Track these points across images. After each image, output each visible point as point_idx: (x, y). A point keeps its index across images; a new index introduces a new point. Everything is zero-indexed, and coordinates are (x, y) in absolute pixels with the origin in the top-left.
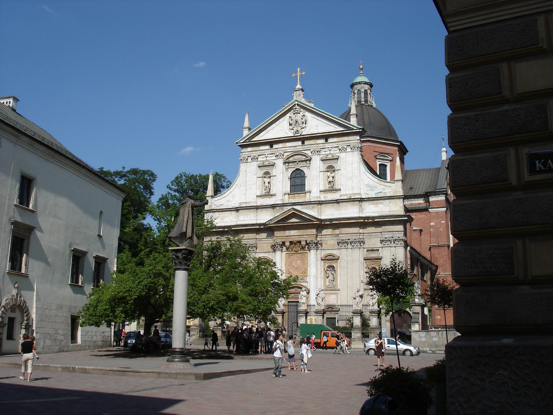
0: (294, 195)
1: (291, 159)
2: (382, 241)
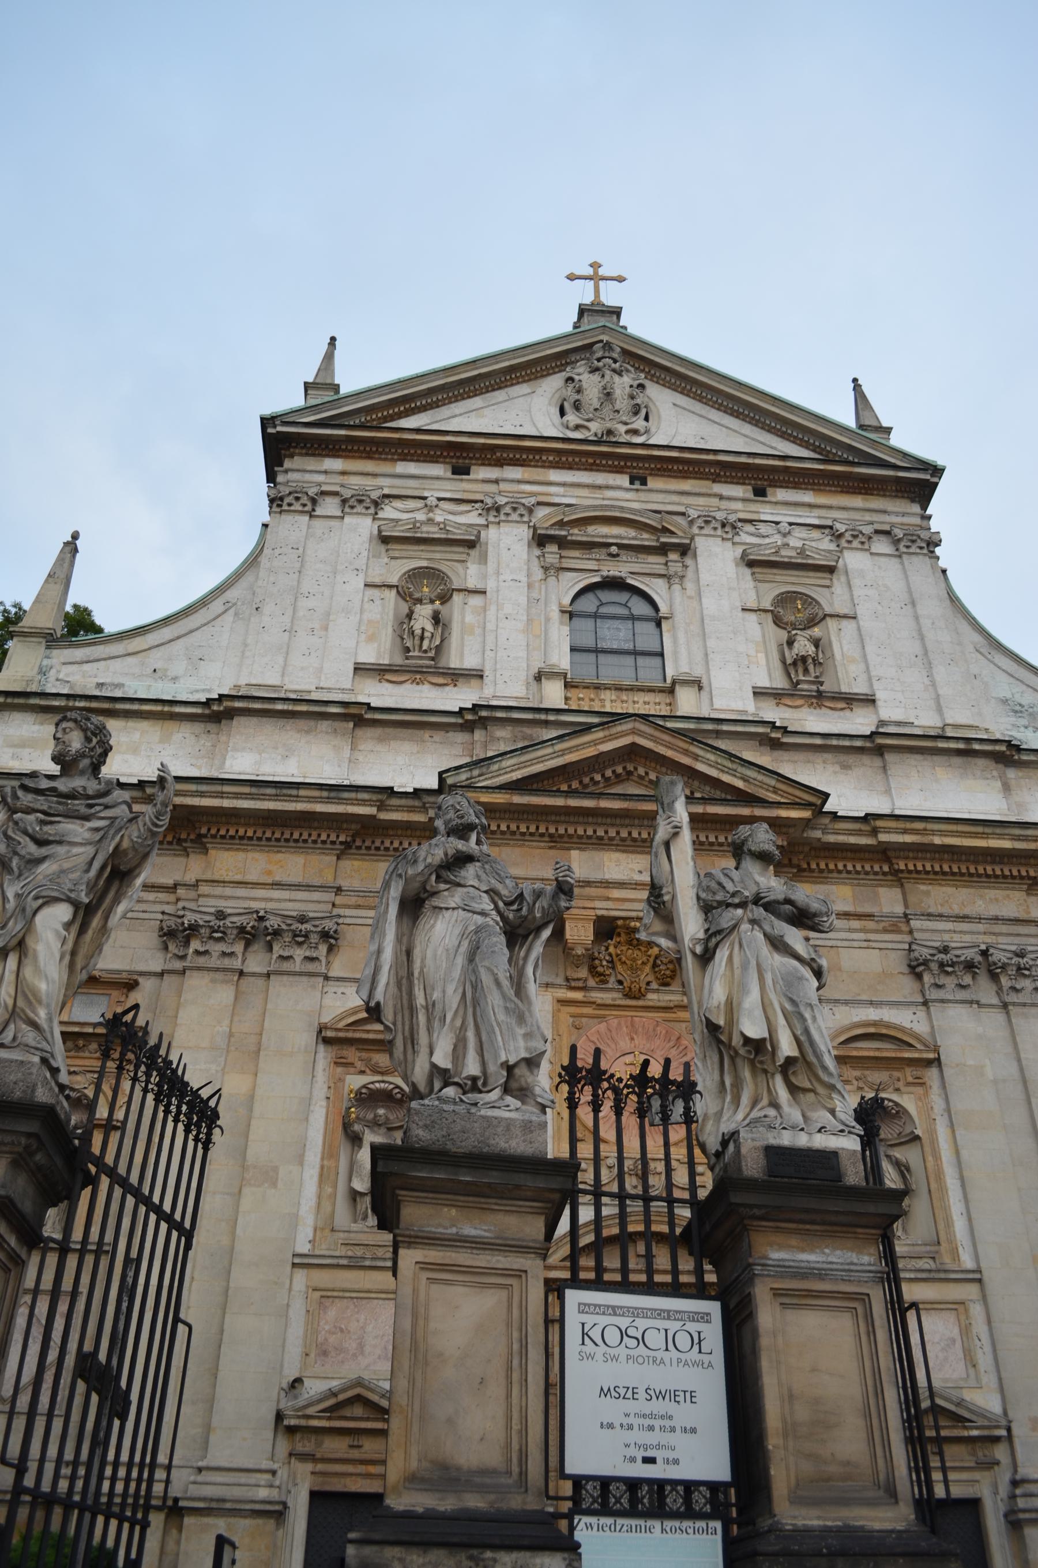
0: (597, 695)
1: (576, 534)
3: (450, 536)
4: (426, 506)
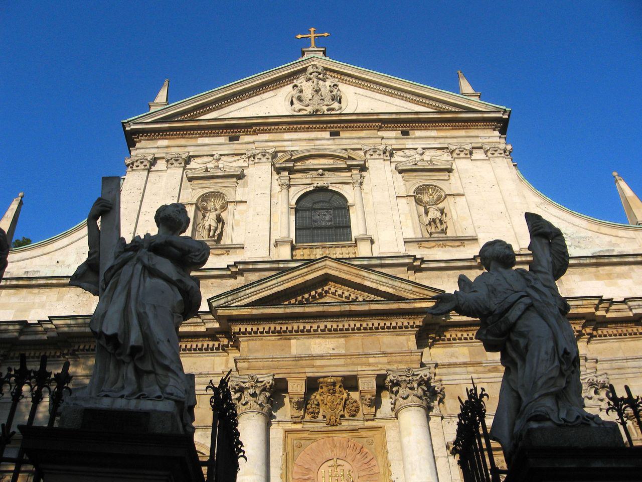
1: (299, 165)
3: (226, 174)
4: (214, 159)
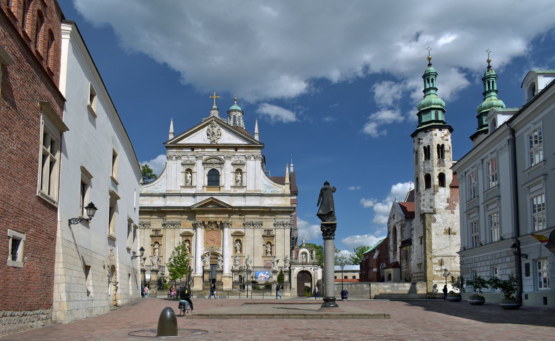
1: (209, 161)
2: (274, 225)
